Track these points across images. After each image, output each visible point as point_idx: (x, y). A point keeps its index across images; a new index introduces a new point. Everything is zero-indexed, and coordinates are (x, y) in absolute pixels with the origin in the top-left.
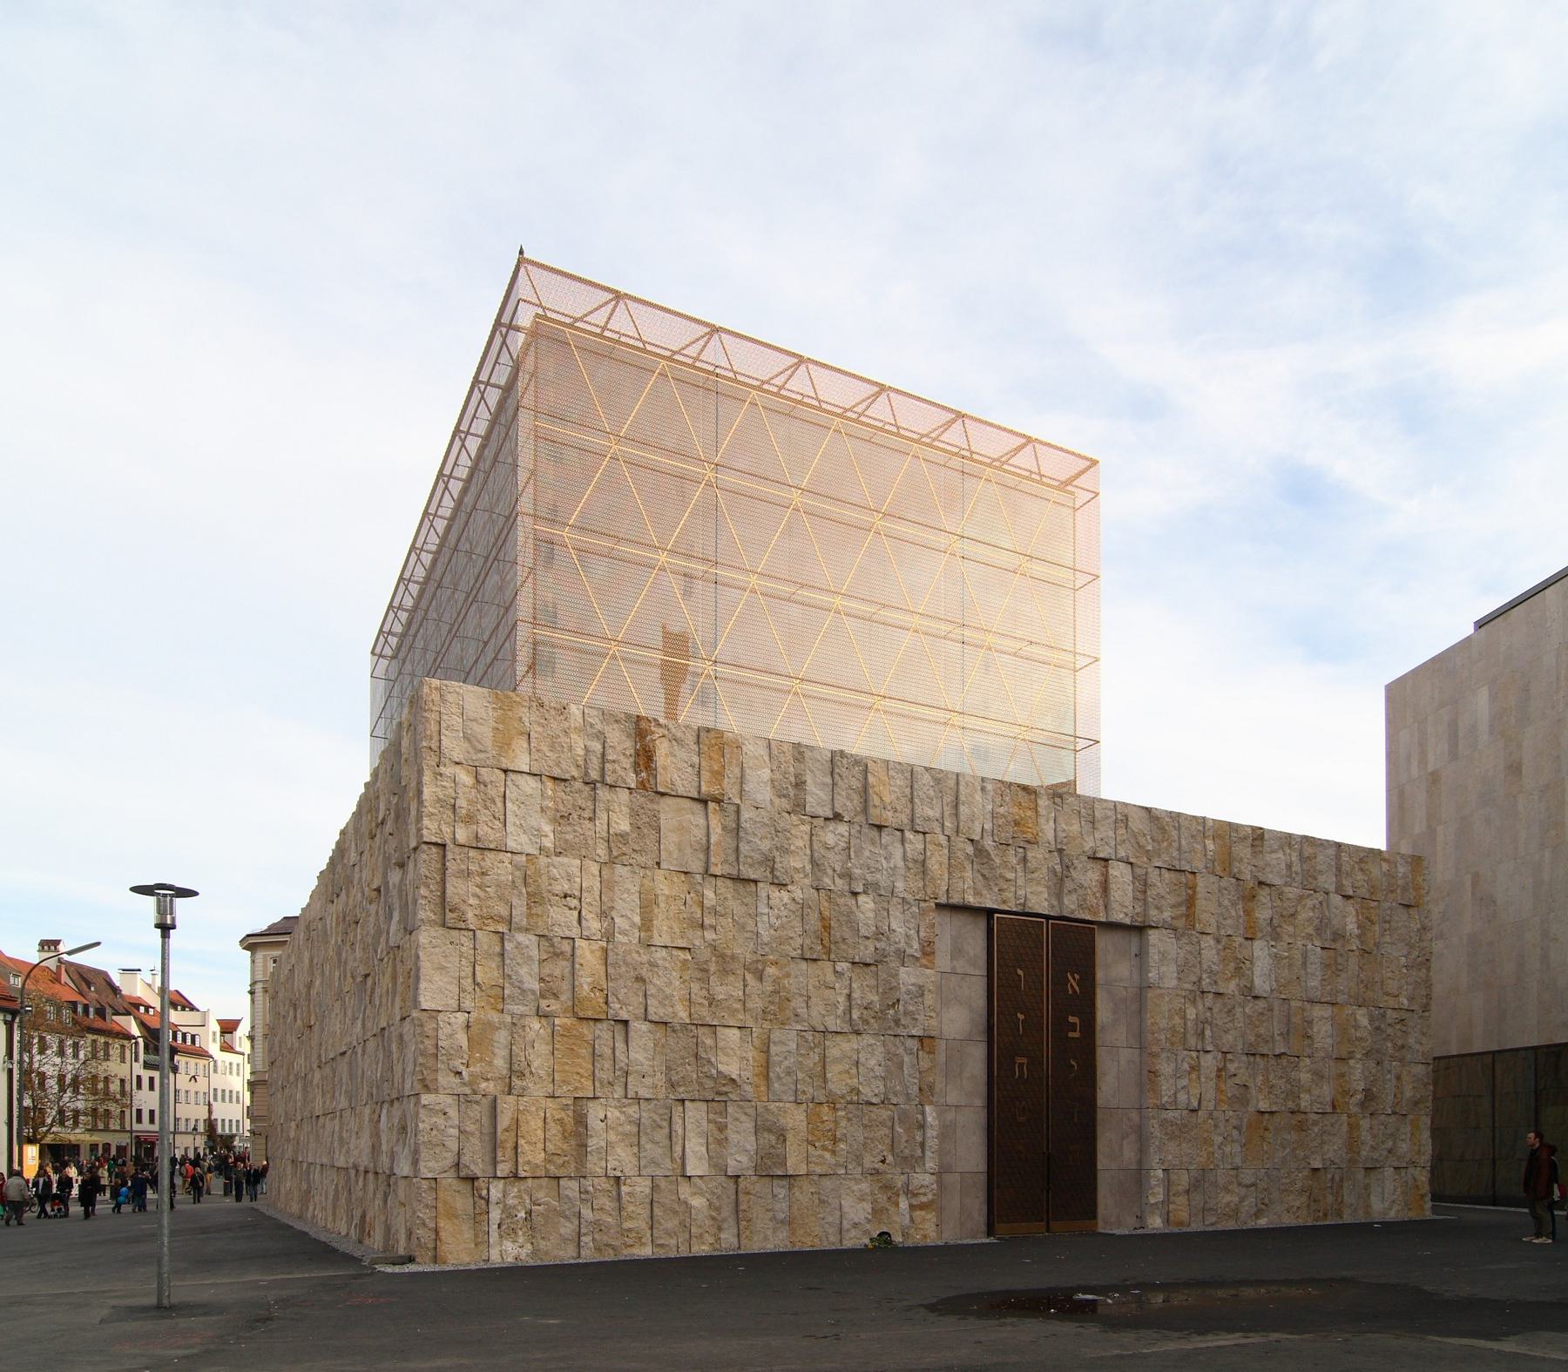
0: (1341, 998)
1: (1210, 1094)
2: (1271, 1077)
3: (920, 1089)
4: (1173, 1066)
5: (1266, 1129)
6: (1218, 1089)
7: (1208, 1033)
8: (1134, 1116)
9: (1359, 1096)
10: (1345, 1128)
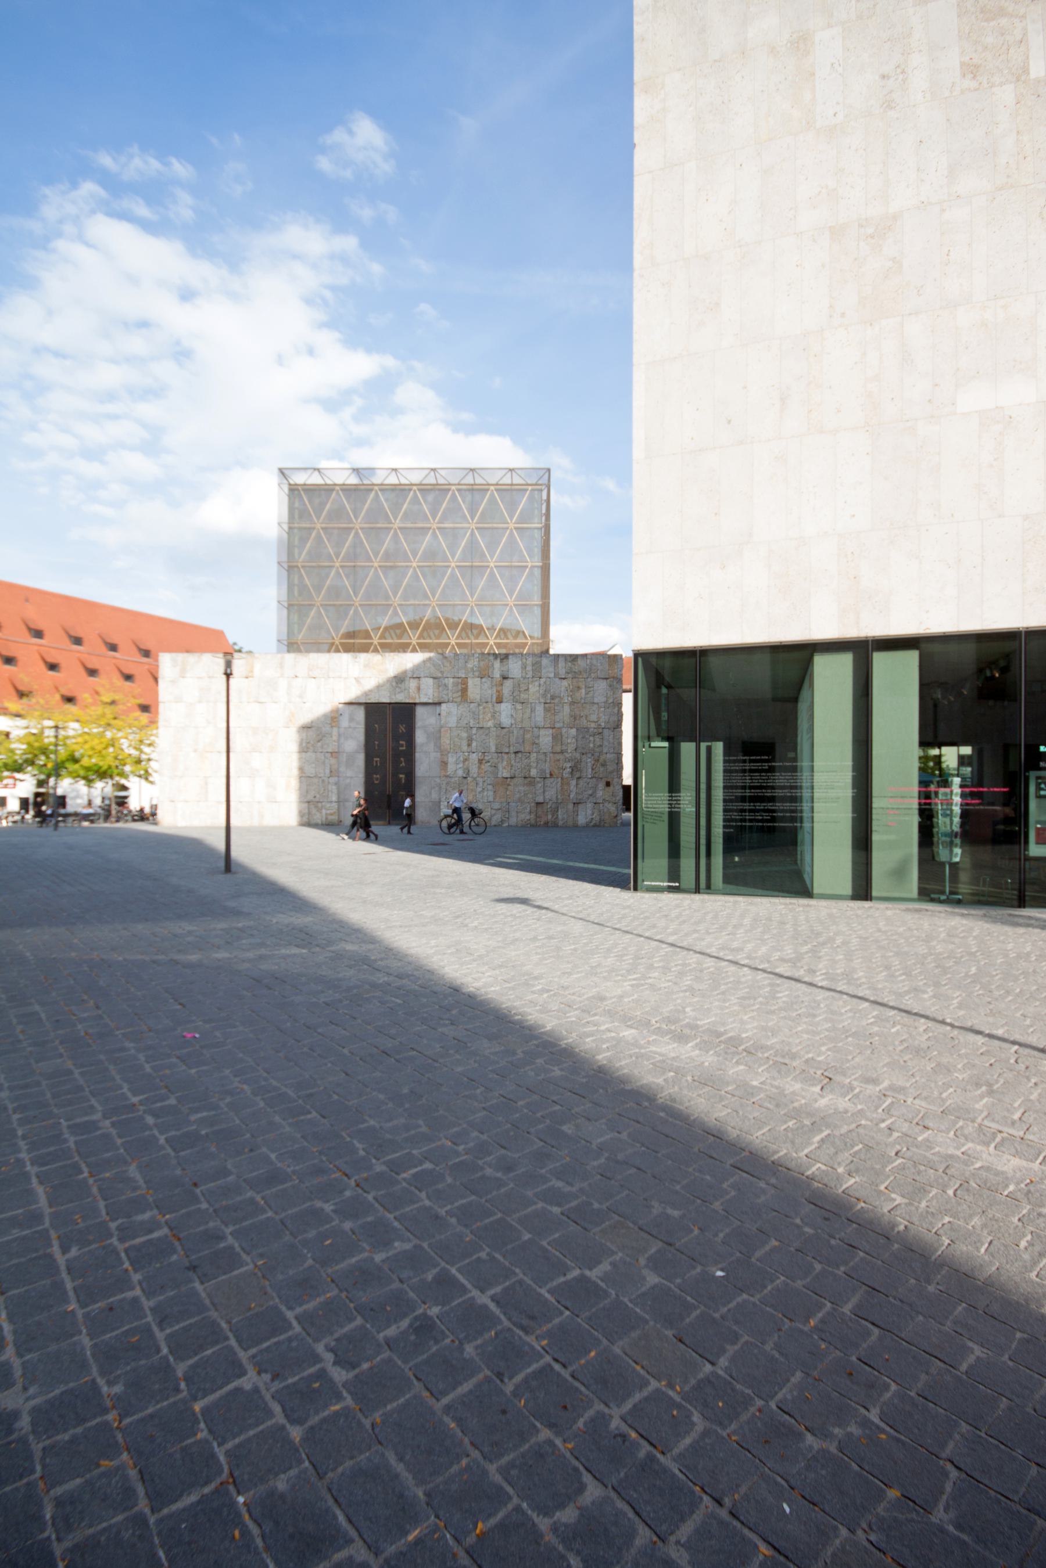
0: (557, 725)
1: (474, 770)
2: (513, 762)
3: (331, 772)
4: (454, 759)
5: (509, 785)
6: (479, 768)
7: (474, 744)
8: (438, 780)
9: (569, 770)
10: (559, 784)
